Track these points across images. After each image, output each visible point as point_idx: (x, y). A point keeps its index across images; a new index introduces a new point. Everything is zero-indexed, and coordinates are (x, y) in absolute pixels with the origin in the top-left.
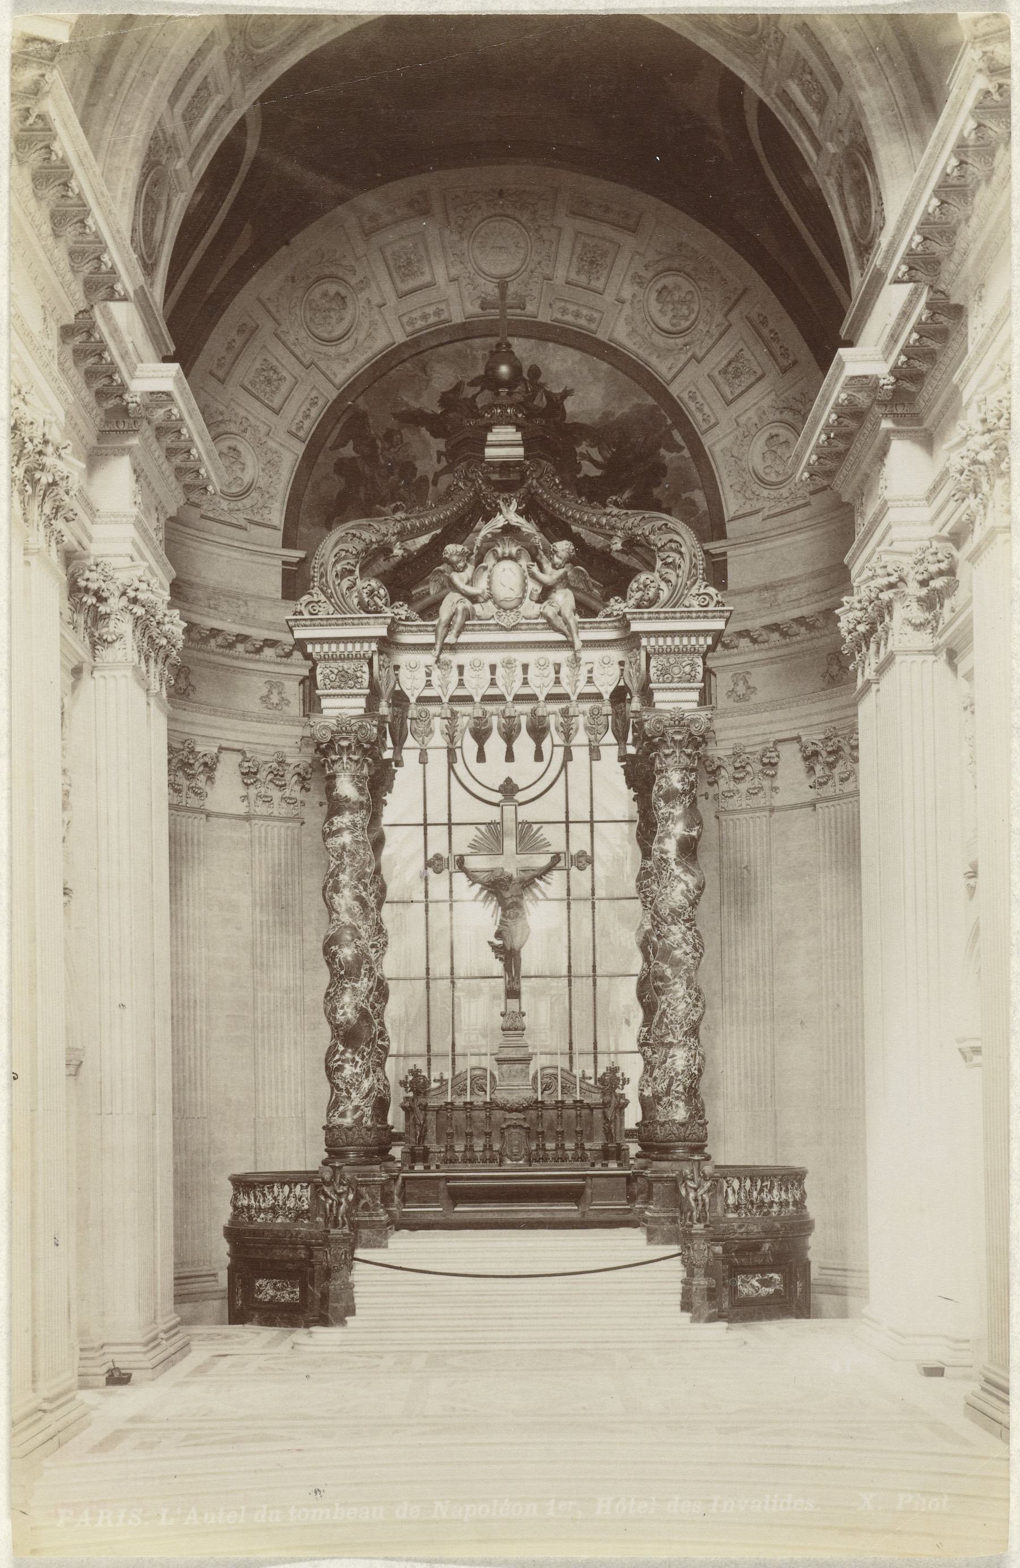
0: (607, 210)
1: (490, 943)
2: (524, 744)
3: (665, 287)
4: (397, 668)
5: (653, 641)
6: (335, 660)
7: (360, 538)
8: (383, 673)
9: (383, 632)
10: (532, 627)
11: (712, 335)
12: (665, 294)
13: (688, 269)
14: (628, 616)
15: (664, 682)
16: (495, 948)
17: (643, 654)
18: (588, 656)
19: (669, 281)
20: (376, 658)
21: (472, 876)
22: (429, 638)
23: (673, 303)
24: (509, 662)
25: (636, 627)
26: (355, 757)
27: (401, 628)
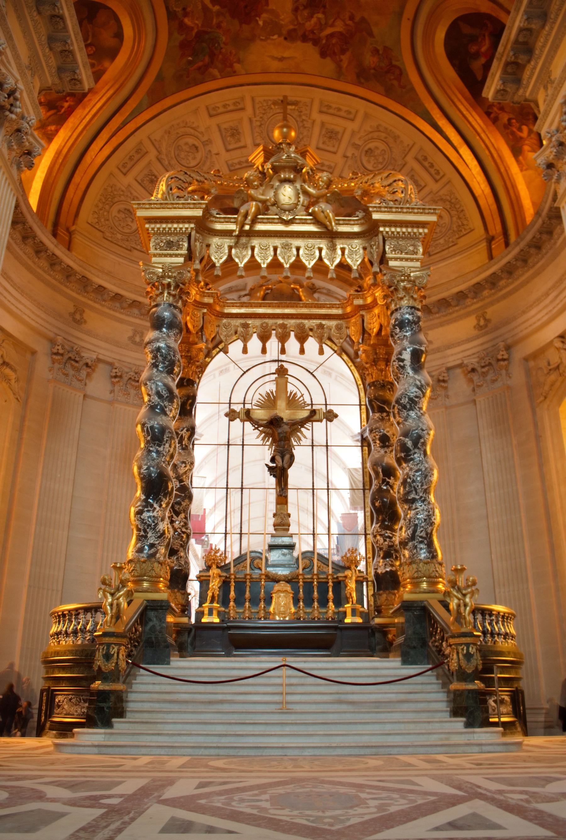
1: (267, 465)
2: (293, 344)
3: (370, 149)
4: (208, 246)
6: (165, 234)
7: (190, 176)
8: (198, 244)
9: (199, 213)
10: (303, 222)
14: (371, 209)
16: (270, 469)
17: (380, 237)
20: (193, 233)
21: (256, 424)
22: (232, 227)
23: (375, 156)
24: (287, 245)
25: (375, 216)
26: (173, 293)
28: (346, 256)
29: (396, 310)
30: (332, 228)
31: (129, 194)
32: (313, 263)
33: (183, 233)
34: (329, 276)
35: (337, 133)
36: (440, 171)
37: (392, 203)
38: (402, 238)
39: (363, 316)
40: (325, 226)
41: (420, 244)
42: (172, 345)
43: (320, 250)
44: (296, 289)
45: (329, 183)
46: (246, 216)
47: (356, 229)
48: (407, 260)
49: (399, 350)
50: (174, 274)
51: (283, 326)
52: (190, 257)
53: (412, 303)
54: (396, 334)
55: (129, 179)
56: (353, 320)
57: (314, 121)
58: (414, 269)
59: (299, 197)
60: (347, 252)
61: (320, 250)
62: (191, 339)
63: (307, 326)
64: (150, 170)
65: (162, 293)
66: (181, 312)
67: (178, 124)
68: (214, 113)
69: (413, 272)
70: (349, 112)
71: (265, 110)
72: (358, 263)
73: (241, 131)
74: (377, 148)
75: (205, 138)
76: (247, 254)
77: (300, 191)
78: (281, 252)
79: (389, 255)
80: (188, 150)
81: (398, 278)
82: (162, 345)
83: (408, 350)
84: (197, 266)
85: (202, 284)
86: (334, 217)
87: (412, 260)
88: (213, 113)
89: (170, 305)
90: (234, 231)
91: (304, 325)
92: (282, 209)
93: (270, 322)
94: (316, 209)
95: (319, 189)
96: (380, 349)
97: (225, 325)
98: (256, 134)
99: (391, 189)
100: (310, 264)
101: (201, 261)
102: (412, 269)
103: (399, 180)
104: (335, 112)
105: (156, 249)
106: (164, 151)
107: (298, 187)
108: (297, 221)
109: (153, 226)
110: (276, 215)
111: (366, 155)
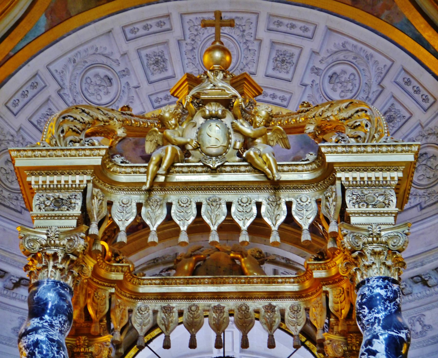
0: (293, 26)
3: (335, 73)
4: (110, 204)
5: (347, 175)
7: (88, 114)
9: (98, 161)
10: (235, 170)
11: (370, 100)
12: (335, 77)
13: (350, 59)
14: (323, 150)
15: (359, 207)
18: (285, 196)
19: (337, 69)
22: (142, 178)
24: (215, 201)
25: (329, 159)
26: (61, 266)
27: (115, 168)
28: (293, 213)
29: (363, 283)
30: (274, 177)
31: (20, 139)
32: (248, 223)
33: (76, 188)
34: (272, 240)
35: (292, 55)
36: (429, 97)
37: (352, 140)
38: (368, 185)
39: (326, 293)
40: (266, 175)
41: (393, 193)
42: (56, 338)
43: (259, 205)
44: (238, 259)
45: (269, 118)
46: (159, 164)
47: (306, 176)
48: (375, 214)
49: (369, 338)
50: (65, 242)
51: (219, 309)
52: (85, 218)
53: (384, 272)
54: (364, 316)
55: (21, 120)
56: (314, 299)
57: (261, 41)
58: (386, 227)
59: (231, 139)
60: (294, 207)
61: (259, 205)
62: (93, 330)
63: (251, 309)
64: (50, 109)
65: (46, 267)
66: (71, 293)
67: (86, 51)
68: (133, 36)
69: (384, 230)
70: (306, 30)
71: (196, 30)
72: (310, 221)
73: (167, 57)
74: (344, 72)
75: (122, 67)
76: (161, 213)
77: (231, 131)
78: (207, 210)
79: (350, 208)
80: (98, 83)
81: (365, 240)
82: (41, 336)
83: (381, 337)
84: (94, 230)
85: (109, 254)
86: (275, 162)
87: (382, 214)
88: (130, 36)
89: (56, 283)
90: (144, 183)
91: (247, 308)
92: (207, 154)
93: (202, 303)
94: (252, 153)
95: (256, 127)
96: (352, 338)
97: (140, 310)
98: (186, 61)
99: (352, 123)
100: (244, 224)
101: (100, 225)
102: (383, 227)
103: (362, 110)
104: (288, 30)
105: (40, 209)
106: (67, 84)
107: (229, 125)
108: (228, 169)
109: (37, 179)
110: (200, 161)
111: (330, 82)
